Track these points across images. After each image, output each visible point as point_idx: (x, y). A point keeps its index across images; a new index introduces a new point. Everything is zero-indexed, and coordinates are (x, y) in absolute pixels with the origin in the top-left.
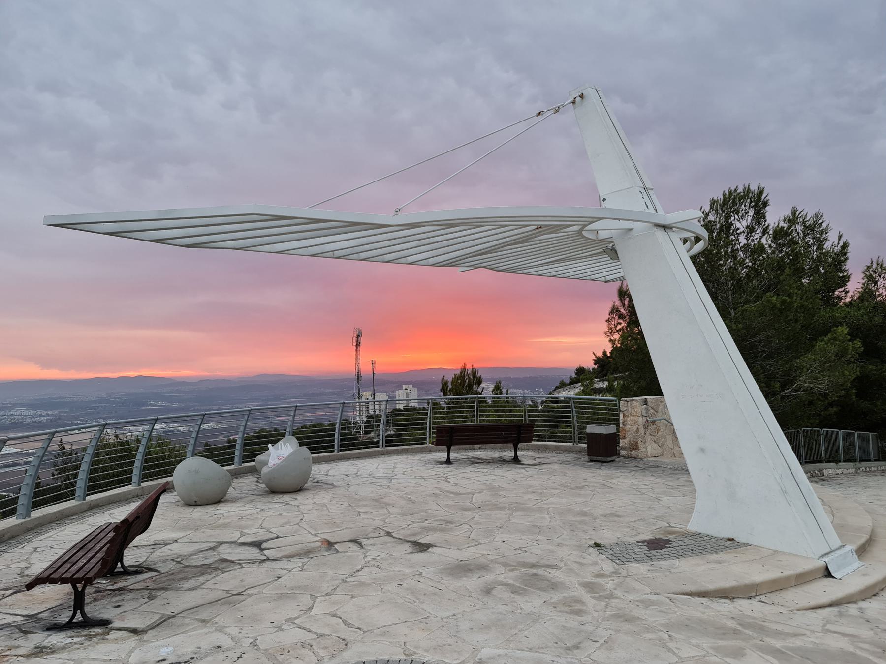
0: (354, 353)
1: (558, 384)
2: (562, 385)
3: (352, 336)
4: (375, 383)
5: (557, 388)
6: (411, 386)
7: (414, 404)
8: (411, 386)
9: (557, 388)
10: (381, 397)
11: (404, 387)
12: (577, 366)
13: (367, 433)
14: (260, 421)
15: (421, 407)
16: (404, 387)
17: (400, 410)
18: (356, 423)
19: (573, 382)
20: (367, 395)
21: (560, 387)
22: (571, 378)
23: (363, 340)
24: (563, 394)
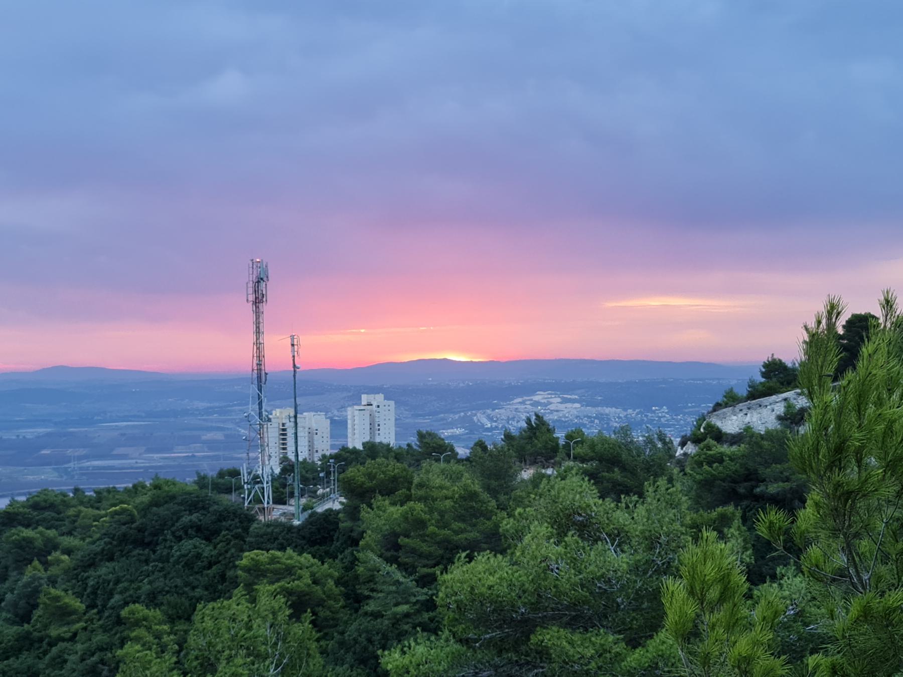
0: (252, 317)
1: (720, 399)
2: (731, 400)
3: (247, 278)
5: (718, 406)
7: (387, 436)
8: (378, 399)
9: (718, 406)
11: (365, 399)
12: (765, 358)
13: (280, 500)
14: (48, 469)
15: (404, 444)
16: (365, 399)
17: (355, 451)
18: (256, 480)
19: (757, 393)
20: (281, 414)
21: (726, 405)
22: (752, 385)
23: (271, 289)
24: (731, 423)
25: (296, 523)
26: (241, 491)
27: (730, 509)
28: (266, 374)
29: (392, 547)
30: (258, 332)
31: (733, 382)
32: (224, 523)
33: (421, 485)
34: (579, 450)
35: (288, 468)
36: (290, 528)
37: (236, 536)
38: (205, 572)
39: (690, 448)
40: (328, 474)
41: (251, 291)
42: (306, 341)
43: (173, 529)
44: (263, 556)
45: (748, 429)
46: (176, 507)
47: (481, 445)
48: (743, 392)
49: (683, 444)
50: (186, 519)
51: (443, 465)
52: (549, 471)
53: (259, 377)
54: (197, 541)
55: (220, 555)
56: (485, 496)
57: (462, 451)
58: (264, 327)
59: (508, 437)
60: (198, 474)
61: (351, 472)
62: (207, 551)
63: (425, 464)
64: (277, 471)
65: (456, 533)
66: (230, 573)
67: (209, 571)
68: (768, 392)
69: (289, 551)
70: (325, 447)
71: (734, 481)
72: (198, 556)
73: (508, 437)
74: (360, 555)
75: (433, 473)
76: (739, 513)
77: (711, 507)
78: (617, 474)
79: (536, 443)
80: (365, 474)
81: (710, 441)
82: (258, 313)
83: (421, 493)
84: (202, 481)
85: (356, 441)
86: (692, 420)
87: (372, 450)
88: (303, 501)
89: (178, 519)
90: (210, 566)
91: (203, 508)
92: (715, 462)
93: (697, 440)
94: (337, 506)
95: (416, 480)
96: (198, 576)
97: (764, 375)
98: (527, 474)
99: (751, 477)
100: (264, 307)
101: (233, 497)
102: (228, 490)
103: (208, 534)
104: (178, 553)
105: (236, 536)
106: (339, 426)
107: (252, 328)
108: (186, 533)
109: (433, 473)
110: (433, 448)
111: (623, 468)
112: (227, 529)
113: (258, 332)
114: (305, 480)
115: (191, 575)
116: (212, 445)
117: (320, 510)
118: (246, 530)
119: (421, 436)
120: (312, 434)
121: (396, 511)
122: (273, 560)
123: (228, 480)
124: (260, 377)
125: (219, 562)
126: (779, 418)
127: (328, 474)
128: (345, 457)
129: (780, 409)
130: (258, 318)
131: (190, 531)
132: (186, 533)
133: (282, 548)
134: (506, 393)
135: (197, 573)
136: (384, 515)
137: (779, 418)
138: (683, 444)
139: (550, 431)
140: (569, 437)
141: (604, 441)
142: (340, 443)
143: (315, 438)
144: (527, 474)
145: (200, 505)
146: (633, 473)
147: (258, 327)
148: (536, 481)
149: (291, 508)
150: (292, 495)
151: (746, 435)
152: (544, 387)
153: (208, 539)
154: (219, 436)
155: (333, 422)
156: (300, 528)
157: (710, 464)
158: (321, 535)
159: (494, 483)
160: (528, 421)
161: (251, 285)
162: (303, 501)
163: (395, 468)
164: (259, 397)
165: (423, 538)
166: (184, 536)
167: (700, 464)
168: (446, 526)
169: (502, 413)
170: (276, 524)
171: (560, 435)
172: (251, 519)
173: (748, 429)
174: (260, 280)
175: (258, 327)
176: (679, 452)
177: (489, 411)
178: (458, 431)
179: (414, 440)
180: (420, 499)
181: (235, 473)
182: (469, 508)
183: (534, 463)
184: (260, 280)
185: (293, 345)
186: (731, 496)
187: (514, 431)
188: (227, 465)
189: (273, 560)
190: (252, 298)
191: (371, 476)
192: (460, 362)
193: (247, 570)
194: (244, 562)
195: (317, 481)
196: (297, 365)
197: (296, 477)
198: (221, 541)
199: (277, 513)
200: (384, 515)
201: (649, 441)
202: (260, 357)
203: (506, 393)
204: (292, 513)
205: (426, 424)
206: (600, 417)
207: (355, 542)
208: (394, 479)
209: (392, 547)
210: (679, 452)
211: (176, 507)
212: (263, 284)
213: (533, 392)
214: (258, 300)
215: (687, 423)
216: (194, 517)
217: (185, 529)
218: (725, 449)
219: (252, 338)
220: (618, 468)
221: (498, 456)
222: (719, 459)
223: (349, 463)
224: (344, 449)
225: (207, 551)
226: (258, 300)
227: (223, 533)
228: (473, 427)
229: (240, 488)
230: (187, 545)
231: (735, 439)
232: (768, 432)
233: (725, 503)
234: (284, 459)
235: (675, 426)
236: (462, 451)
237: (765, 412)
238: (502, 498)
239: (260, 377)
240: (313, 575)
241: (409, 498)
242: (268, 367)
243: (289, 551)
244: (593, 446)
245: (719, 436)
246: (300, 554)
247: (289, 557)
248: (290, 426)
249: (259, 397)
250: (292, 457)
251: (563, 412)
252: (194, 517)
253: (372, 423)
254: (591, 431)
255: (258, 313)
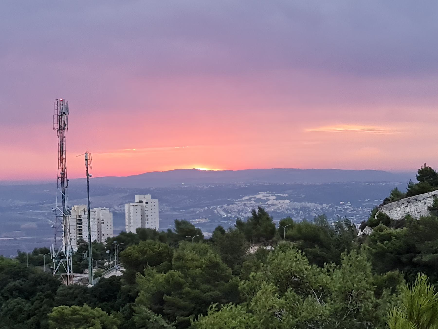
0: (57, 140)
1: (388, 196)
2: (396, 196)
4: (93, 191)
5: (387, 201)
6: (148, 196)
7: (153, 224)
8: (148, 196)
9: (387, 201)
10: (101, 213)
12: (419, 167)
13: (78, 270)
15: (165, 229)
17: (131, 234)
18: (61, 256)
19: (414, 192)
20: (78, 209)
21: (393, 200)
24: (396, 213)
25: (90, 286)
26: (50, 264)
27: (396, 272)
28: (68, 180)
29: (158, 303)
30: (62, 151)
31: (397, 184)
32: (39, 287)
33: (179, 258)
34: (290, 232)
35: (83, 247)
36: (85, 290)
37: (47, 296)
38: (25, 322)
39: (368, 231)
40: (112, 251)
41: (56, 121)
42: (95, 157)
43: (3, 291)
44: (67, 310)
45: (408, 216)
46: (5, 276)
47: (220, 229)
48: (404, 190)
49: (362, 228)
50: (11, 284)
51: (193, 244)
52: (269, 248)
53: (63, 183)
54: (19, 299)
55: (37, 309)
56: (224, 266)
57: (207, 235)
58: (66, 147)
59: (239, 224)
60: (19, 252)
61: (129, 249)
62: (27, 307)
63: (181, 244)
64: (76, 249)
65: (204, 292)
66: (43, 322)
67: (28, 321)
68: (421, 190)
69: (85, 306)
70: (109, 232)
71: (399, 253)
72: (20, 310)
73: (239, 224)
74: (134, 308)
75: (187, 250)
76: (402, 276)
77: (383, 271)
78: (317, 249)
79: (260, 227)
80: (138, 251)
81: (381, 225)
82: (61, 138)
83: (179, 263)
84: (22, 257)
85: (131, 228)
86: (368, 211)
87: (143, 233)
88: (95, 270)
89: (5, 285)
90: (29, 317)
91: (24, 276)
92: (385, 240)
93: (372, 225)
94: (119, 274)
95: (175, 254)
96: (20, 324)
97: (419, 178)
98: (253, 250)
99: (411, 250)
100: (66, 133)
101: (45, 268)
102: (41, 264)
103: (27, 295)
104: (6, 308)
105: (47, 296)
106: (119, 217)
107: (58, 148)
108: (12, 294)
109: (187, 250)
110: (186, 232)
111: (321, 245)
112: (41, 291)
113: (62, 151)
114: (95, 256)
115: (16, 324)
116: (28, 231)
117: (107, 276)
118: (55, 291)
119: (178, 223)
120: (100, 223)
121: (161, 277)
122: (74, 312)
123: (42, 256)
124: (64, 183)
125: (35, 314)
126: (429, 209)
127: (112, 251)
128: (124, 239)
129: (430, 202)
130: (61, 141)
131: (14, 293)
132: (12, 294)
133: (80, 304)
134: (237, 193)
135: (19, 322)
136: (153, 280)
137: (429, 209)
138: (362, 228)
139: (269, 219)
140: (282, 223)
141: (308, 226)
142: (119, 229)
143: (102, 226)
144: (253, 250)
145: (22, 274)
146: (328, 248)
147: (62, 147)
148: (261, 254)
149: (86, 275)
150: (86, 267)
151: (407, 220)
152: (264, 189)
153: (27, 298)
154: (34, 225)
155: (115, 214)
156: (93, 289)
157: (382, 241)
158: (107, 294)
159: (230, 257)
160: (254, 212)
161: (56, 117)
162: (95, 270)
163: (159, 246)
164: (63, 197)
165: (181, 296)
166: (10, 296)
167: (375, 242)
168: (194, 286)
169: (234, 207)
170: (76, 286)
171: (276, 222)
172: (58, 284)
173: (408, 216)
174: (62, 114)
175: (62, 147)
176: (360, 233)
177: (225, 206)
178: (203, 220)
179: (172, 227)
180: (178, 268)
181: (46, 251)
182: (212, 273)
183: (258, 242)
184: (62, 114)
185: (86, 160)
186: (397, 264)
187: (243, 220)
188: (40, 246)
189: (74, 312)
190: (57, 126)
191: (143, 252)
192: (205, 171)
193: (55, 319)
194: (54, 314)
195: (104, 256)
196: (90, 174)
197: (89, 254)
198: (37, 299)
199: (76, 279)
200: (153, 280)
201: (339, 226)
202: (63, 169)
203: (237, 193)
204: (87, 278)
205: (181, 216)
206: (304, 209)
207: (132, 299)
208: (160, 254)
209: (158, 303)
210: (360, 233)
211: (5, 276)
212: (65, 117)
213: (257, 193)
214: (62, 128)
215: (364, 213)
216: (17, 283)
217: (11, 291)
218: (392, 230)
219: (58, 155)
220: (321, 244)
221: (234, 236)
222: (389, 237)
223: (127, 244)
224: (123, 233)
225: (27, 307)
226: (62, 128)
227: (38, 293)
228: (213, 217)
229: (49, 262)
230: (12, 302)
231: (399, 224)
232: (422, 218)
233: (392, 269)
234: (80, 241)
235: (357, 215)
236: (207, 235)
237: (420, 204)
238: (236, 266)
239: (64, 183)
240: (102, 322)
241: (170, 267)
242: (69, 175)
243: (85, 306)
244: (300, 230)
245: (388, 221)
246: (93, 308)
247: (86, 310)
248: (84, 217)
249: (63, 197)
250: (86, 239)
251: (278, 206)
252: (17, 283)
253: (145, 215)
254: (298, 219)
255: (61, 138)
